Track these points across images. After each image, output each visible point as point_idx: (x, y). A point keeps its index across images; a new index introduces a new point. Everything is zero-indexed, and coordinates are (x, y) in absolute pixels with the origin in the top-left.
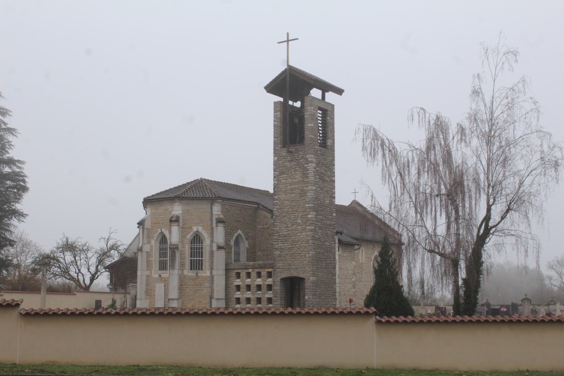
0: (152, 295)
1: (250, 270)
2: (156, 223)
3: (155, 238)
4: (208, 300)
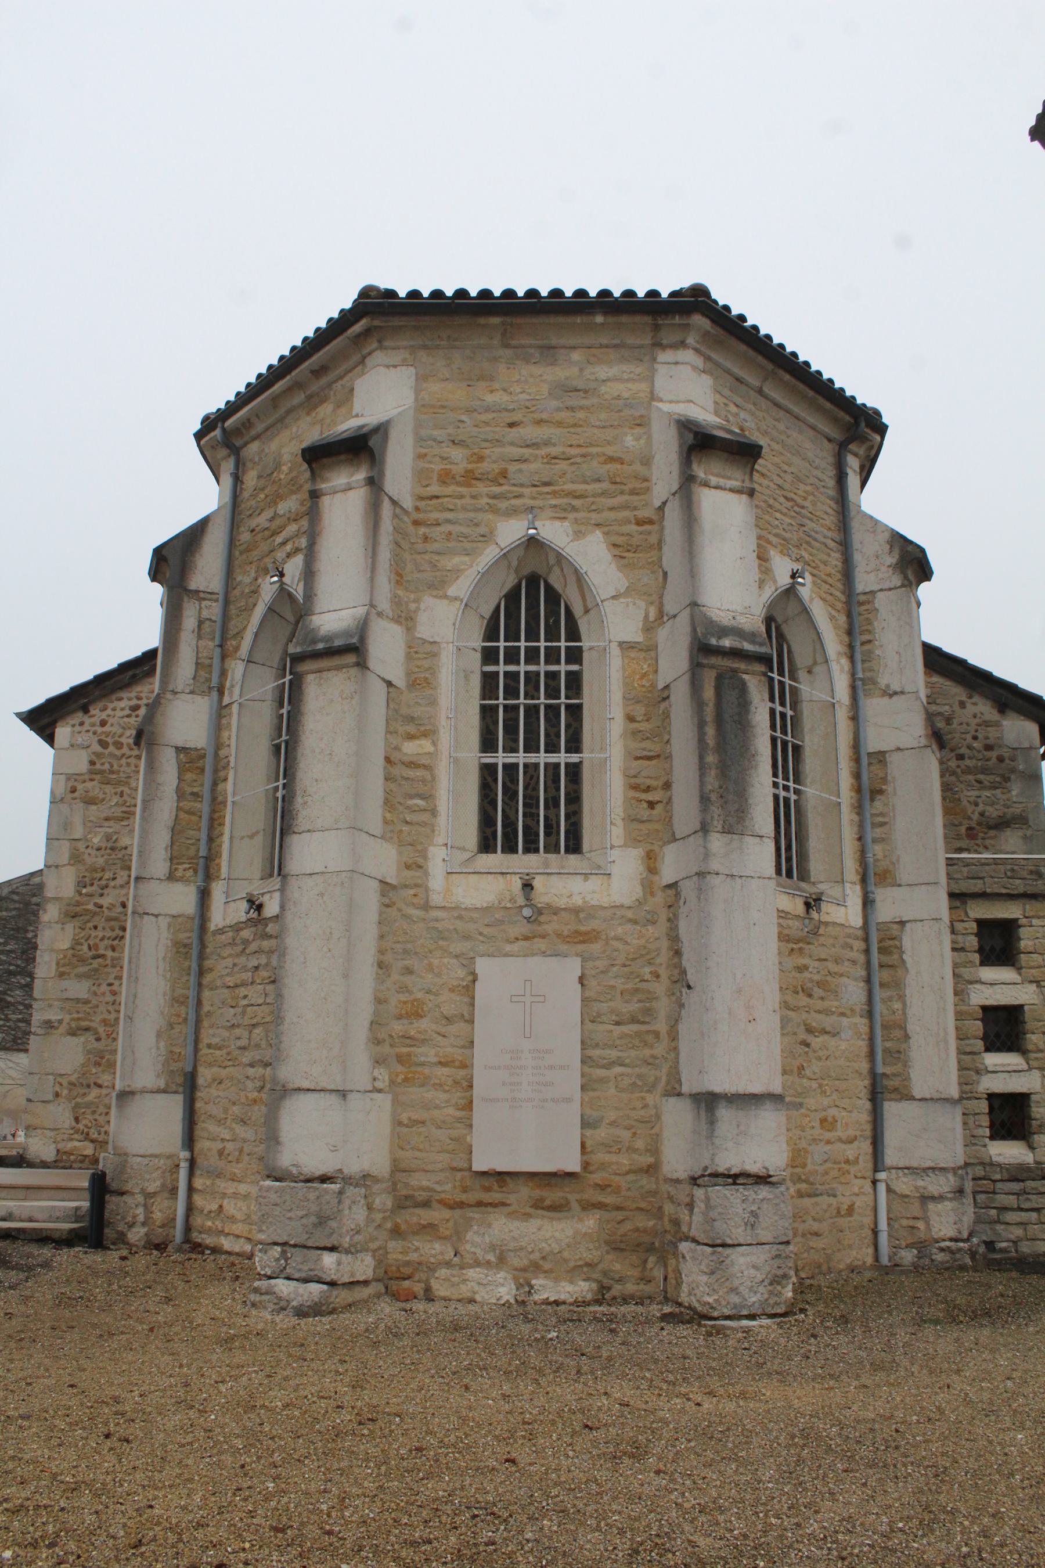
0: (427, 1054)
2: (470, 477)
3: (462, 587)
4: (862, 1115)
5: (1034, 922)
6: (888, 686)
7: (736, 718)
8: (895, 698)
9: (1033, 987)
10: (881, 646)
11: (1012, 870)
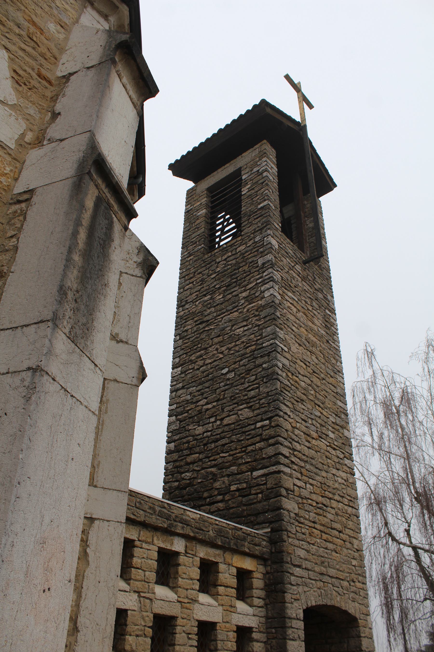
1: (178, 545)
5: (144, 545)
6: (117, 334)
7: (102, 242)
8: (121, 344)
9: (135, 596)
10: (119, 307)
11: (140, 503)
